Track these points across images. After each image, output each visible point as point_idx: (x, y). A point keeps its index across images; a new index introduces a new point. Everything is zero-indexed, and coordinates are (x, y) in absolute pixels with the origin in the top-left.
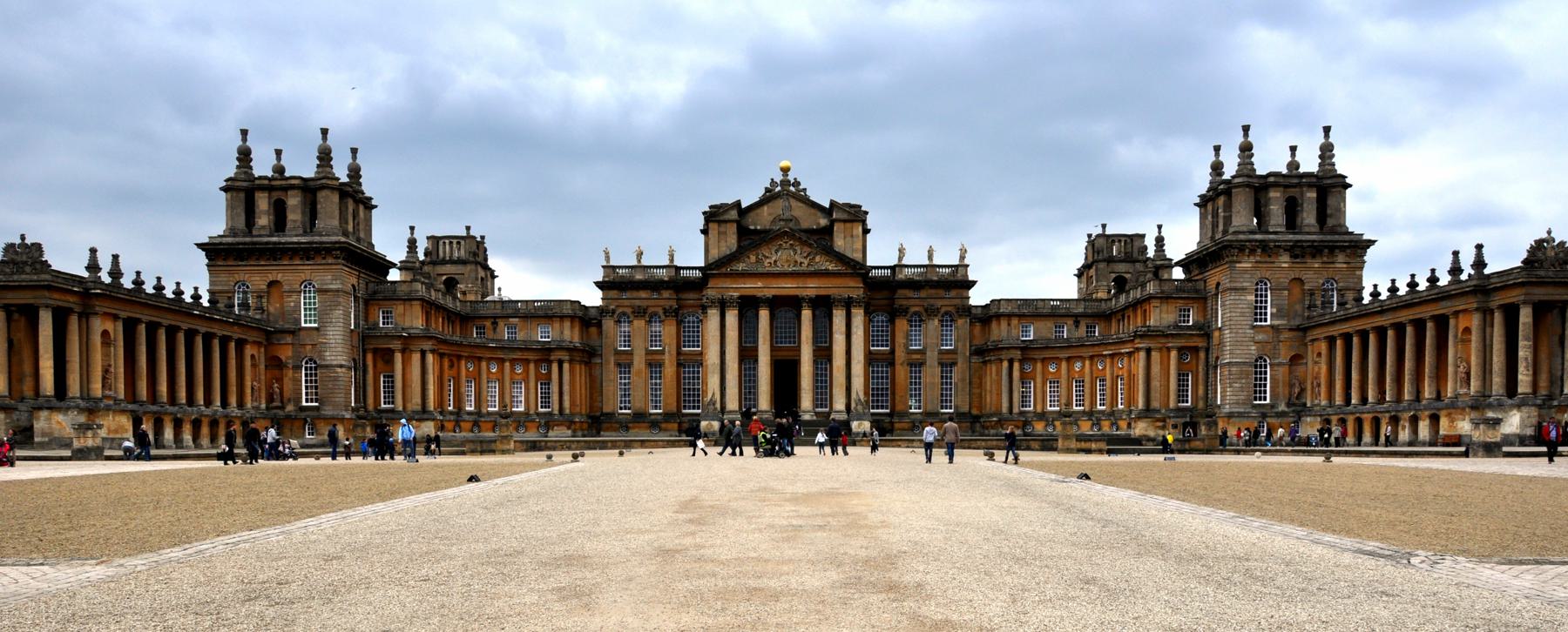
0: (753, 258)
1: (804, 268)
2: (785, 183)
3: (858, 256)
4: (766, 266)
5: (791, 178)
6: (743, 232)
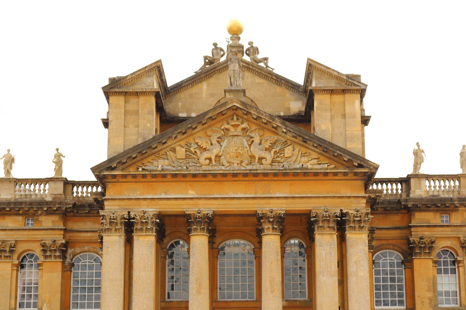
0: (181, 152)
1: (266, 166)
2: (236, 49)
3: (352, 147)
4: (203, 163)
5: (244, 42)
6: (167, 121)
